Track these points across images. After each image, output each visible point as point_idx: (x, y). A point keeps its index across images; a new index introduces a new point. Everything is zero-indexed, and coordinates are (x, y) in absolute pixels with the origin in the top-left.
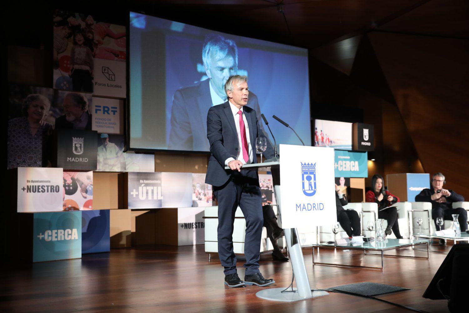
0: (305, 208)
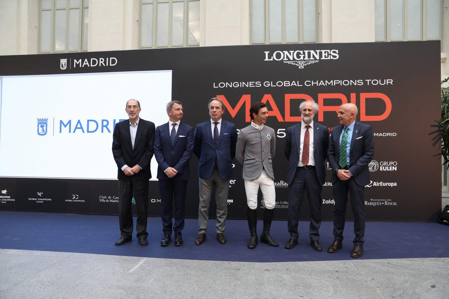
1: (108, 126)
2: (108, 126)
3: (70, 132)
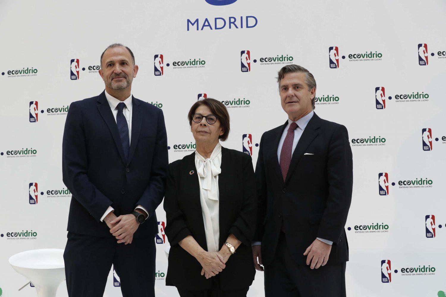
0: (209, 25)
1: (235, 23)
2: (235, 23)
3: (198, 29)
